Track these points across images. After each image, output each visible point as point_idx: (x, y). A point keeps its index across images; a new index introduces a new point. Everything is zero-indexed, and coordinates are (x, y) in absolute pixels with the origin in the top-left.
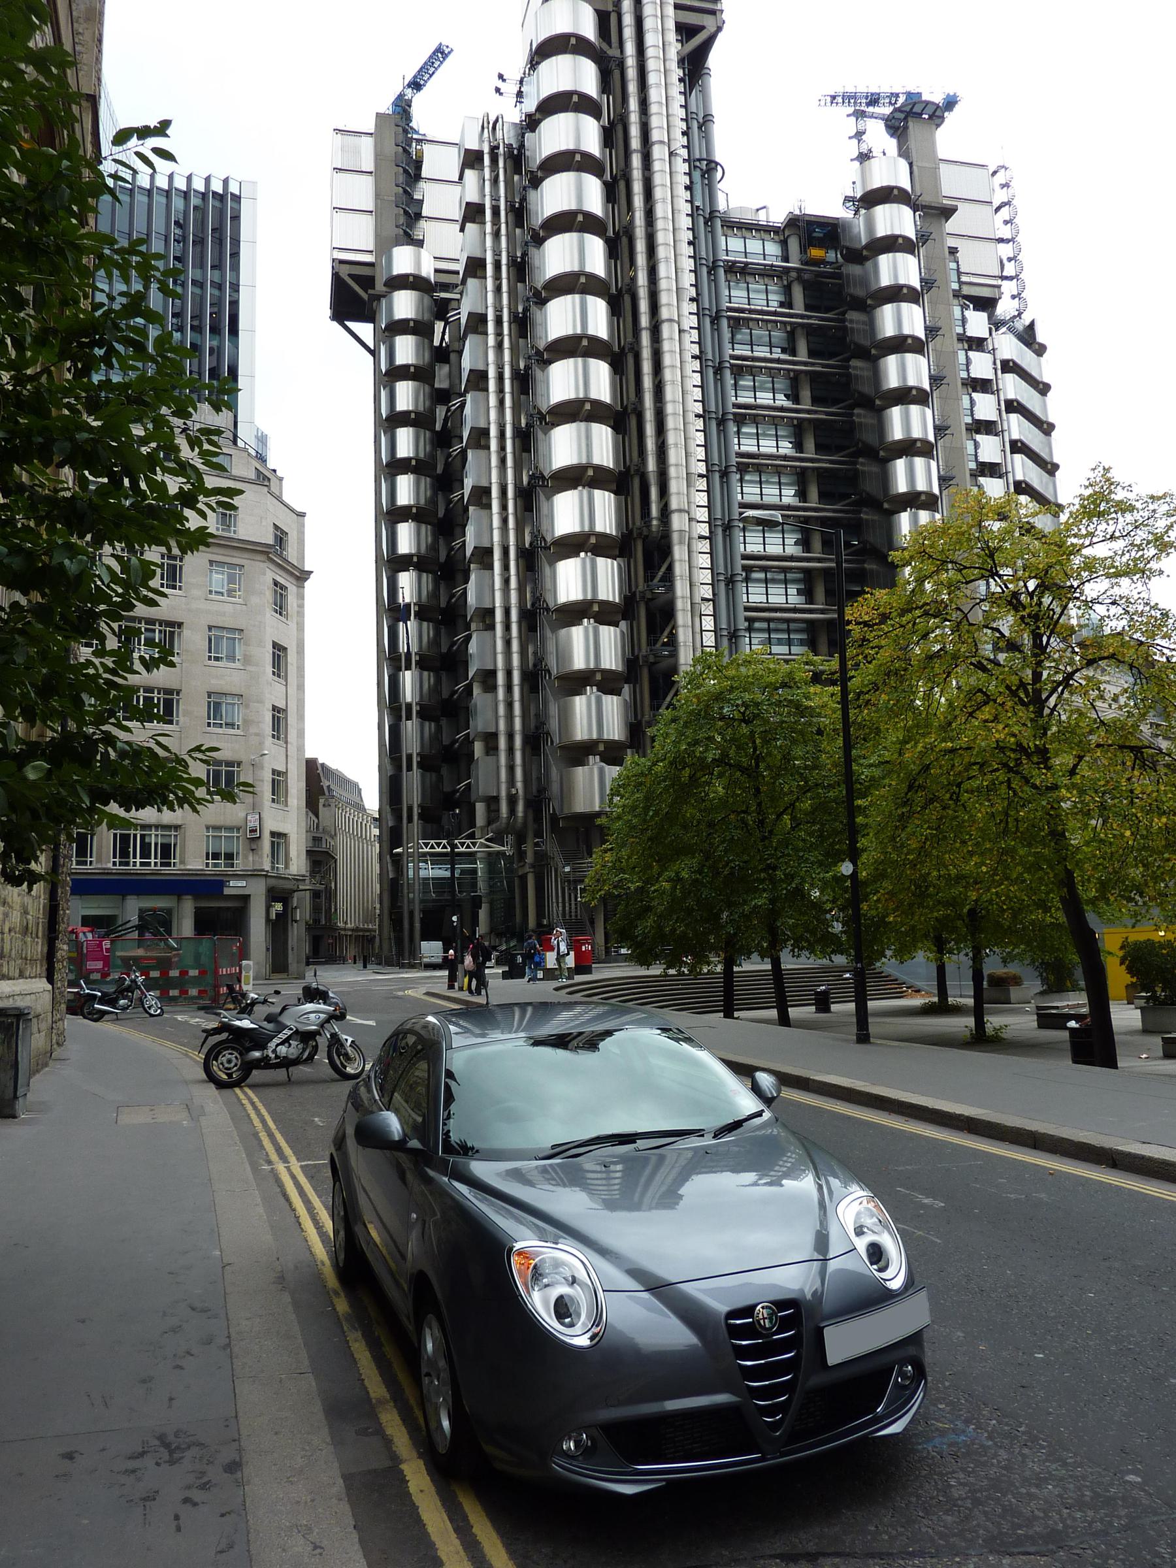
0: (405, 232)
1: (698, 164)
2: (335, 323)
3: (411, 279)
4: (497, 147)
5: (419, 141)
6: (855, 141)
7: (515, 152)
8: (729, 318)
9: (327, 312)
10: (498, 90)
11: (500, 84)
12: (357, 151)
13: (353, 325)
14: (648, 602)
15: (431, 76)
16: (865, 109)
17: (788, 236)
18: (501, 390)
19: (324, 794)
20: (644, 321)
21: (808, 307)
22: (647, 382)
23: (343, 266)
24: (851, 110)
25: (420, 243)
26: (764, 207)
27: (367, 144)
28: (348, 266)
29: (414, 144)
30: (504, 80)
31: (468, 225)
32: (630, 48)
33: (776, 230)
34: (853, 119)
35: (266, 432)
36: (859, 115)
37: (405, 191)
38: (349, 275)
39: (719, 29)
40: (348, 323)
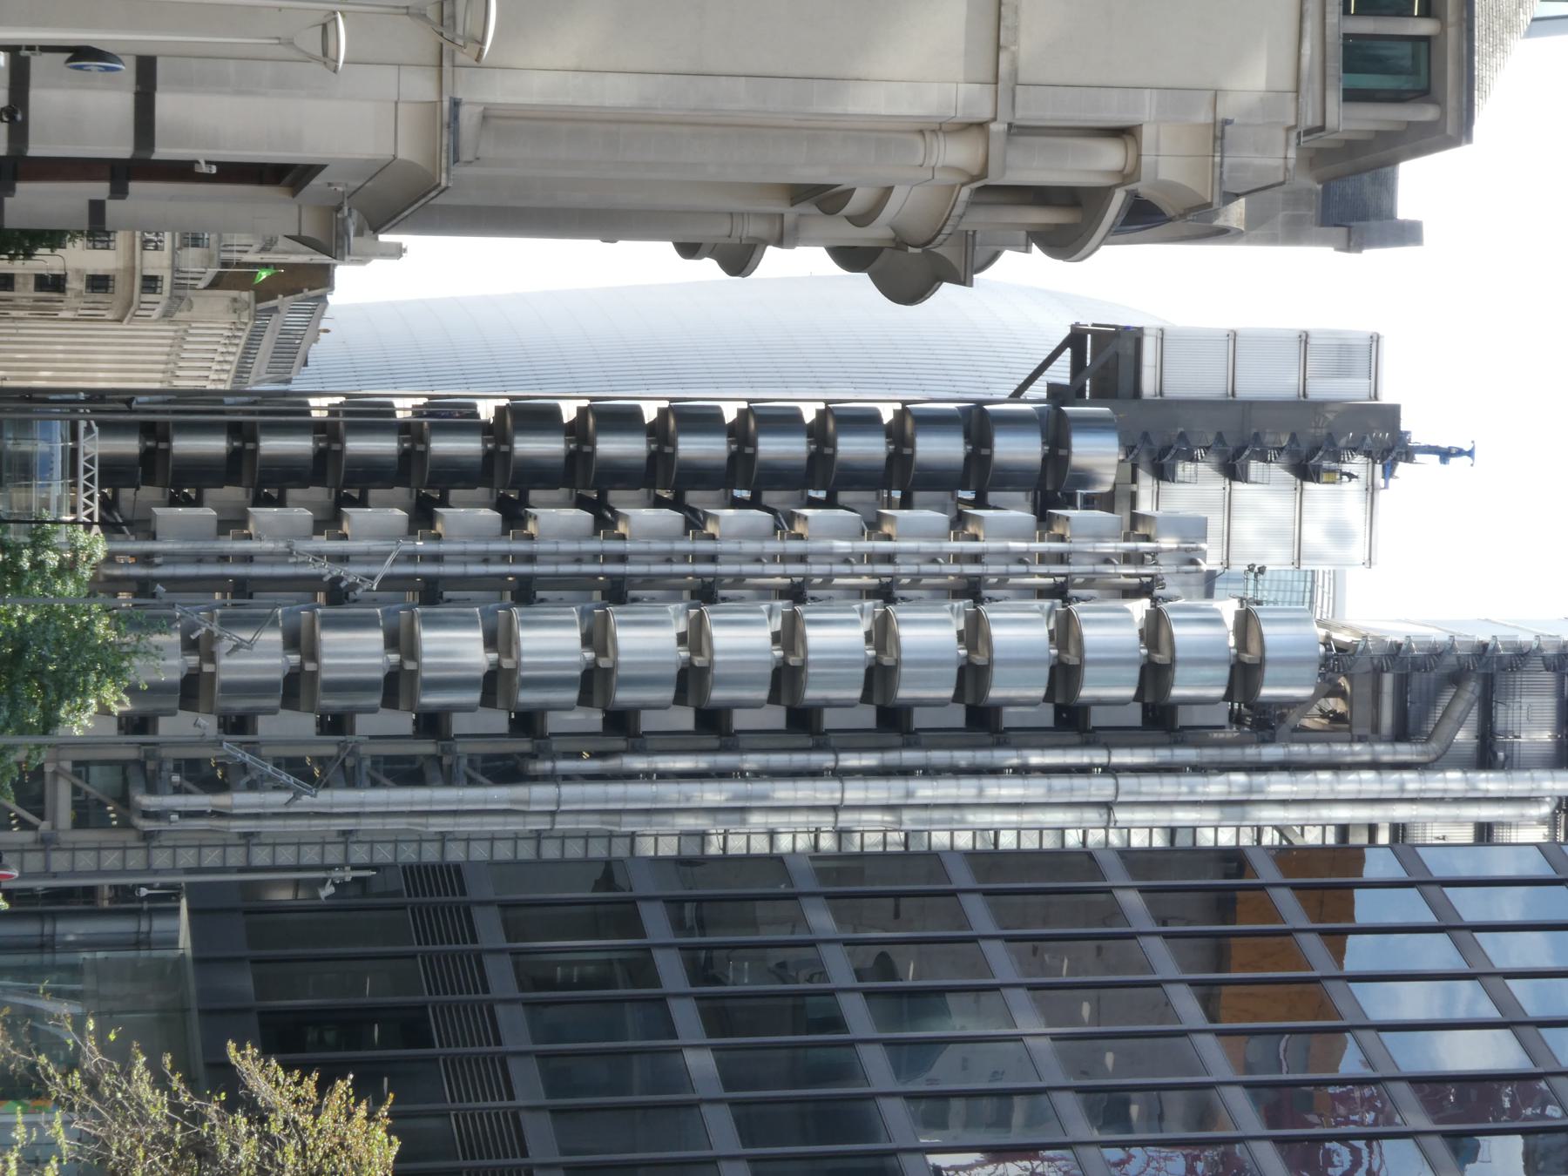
2: (1067, 332)
9: (1087, 320)
11: (1256, 569)
12: (1343, 371)
14: (437, 759)
19: (258, 300)
23: (1130, 346)
28: (1131, 351)
40: (1069, 350)
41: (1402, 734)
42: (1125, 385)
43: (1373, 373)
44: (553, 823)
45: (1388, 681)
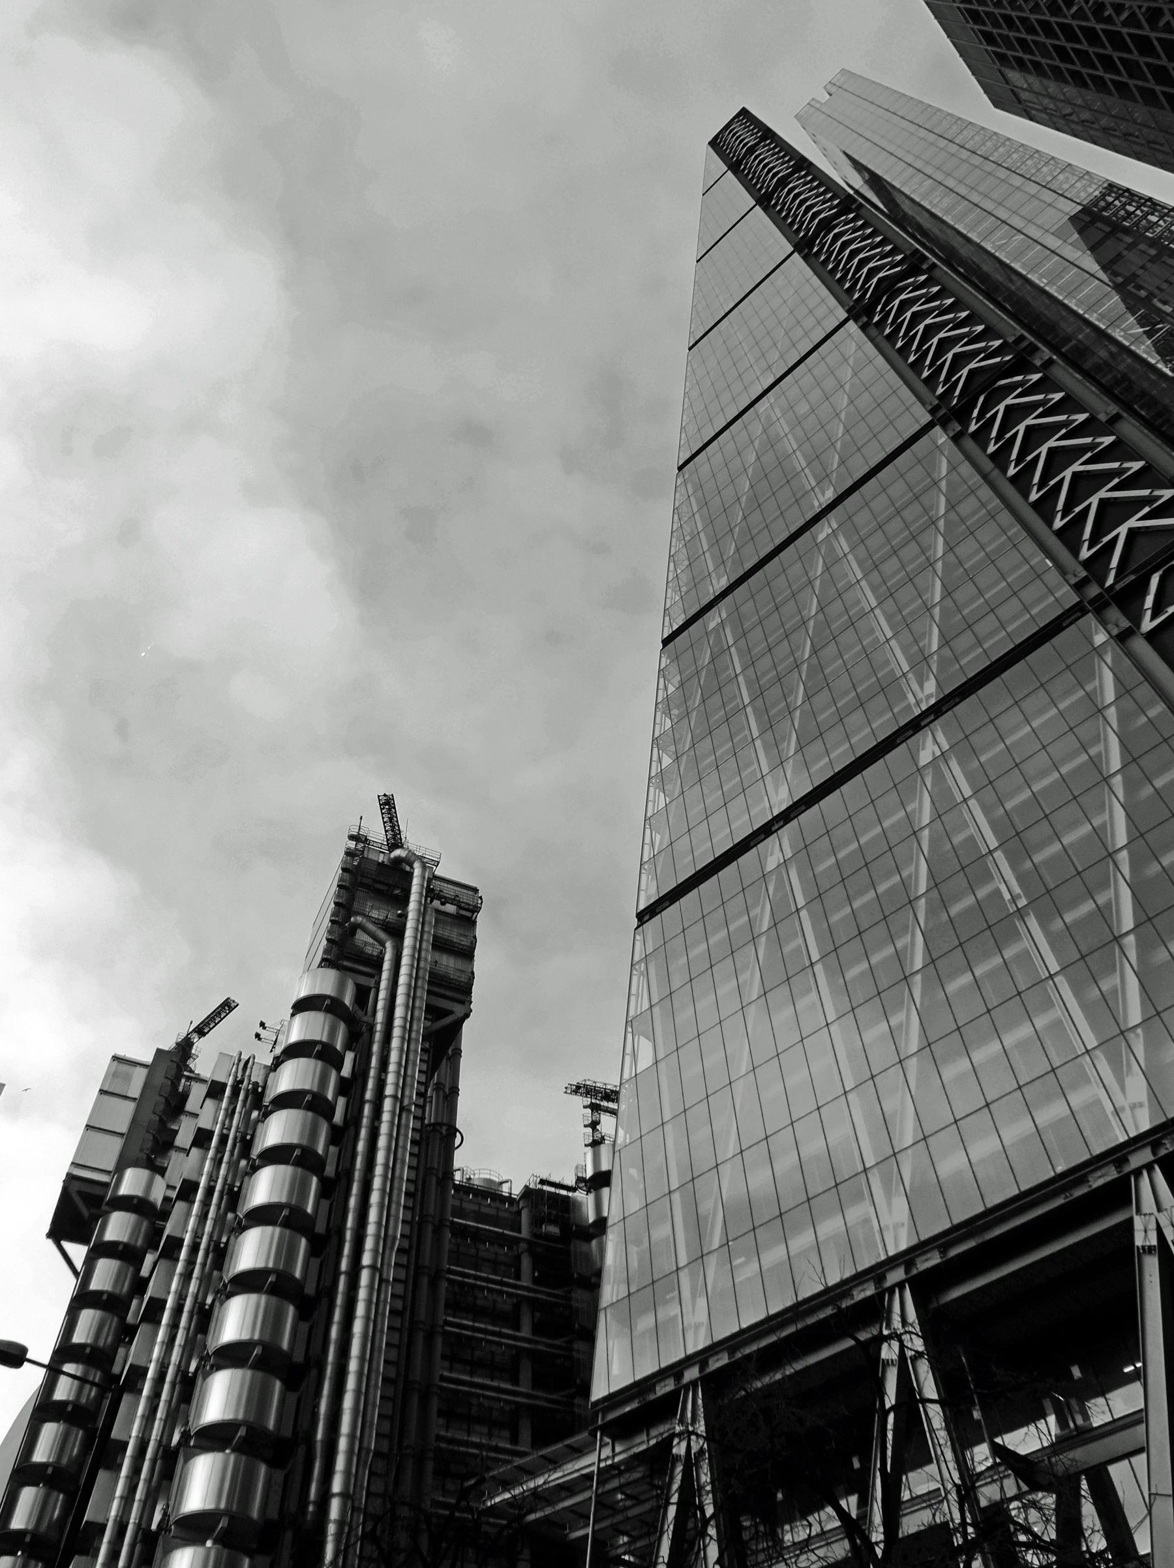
0: (149, 1158)
1: (438, 1128)
3: (135, 1201)
4: (242, 1082)
5: (188, 1078)
6: (589, 1130)
7: (260, 1090)
8: (449, 1280)
10: (258, 1036)
11: (260, 1030)
12: (128, 1078)
13: (67, 1245)
15: (216, 1024)
16: (602, 1103)
18: (174, 1326)
20: (344, 1265)
21: (535, 1281)
22: (334, 1332)
24: (588, 1101)
25: (162, 1171)
26: (507, 1182)
27: (140, 1075)
29: (183, 1081)
30: (264, 1028)
31: (193, 1149)
32: (380, 1017)
34: (589, 1111)
36: (595, 1108)
37: (161, 1120)
39: (467, 1016)
41: (377, 963)
42: (97, 1191)
44: (359, 1509)
45: (346, 963)
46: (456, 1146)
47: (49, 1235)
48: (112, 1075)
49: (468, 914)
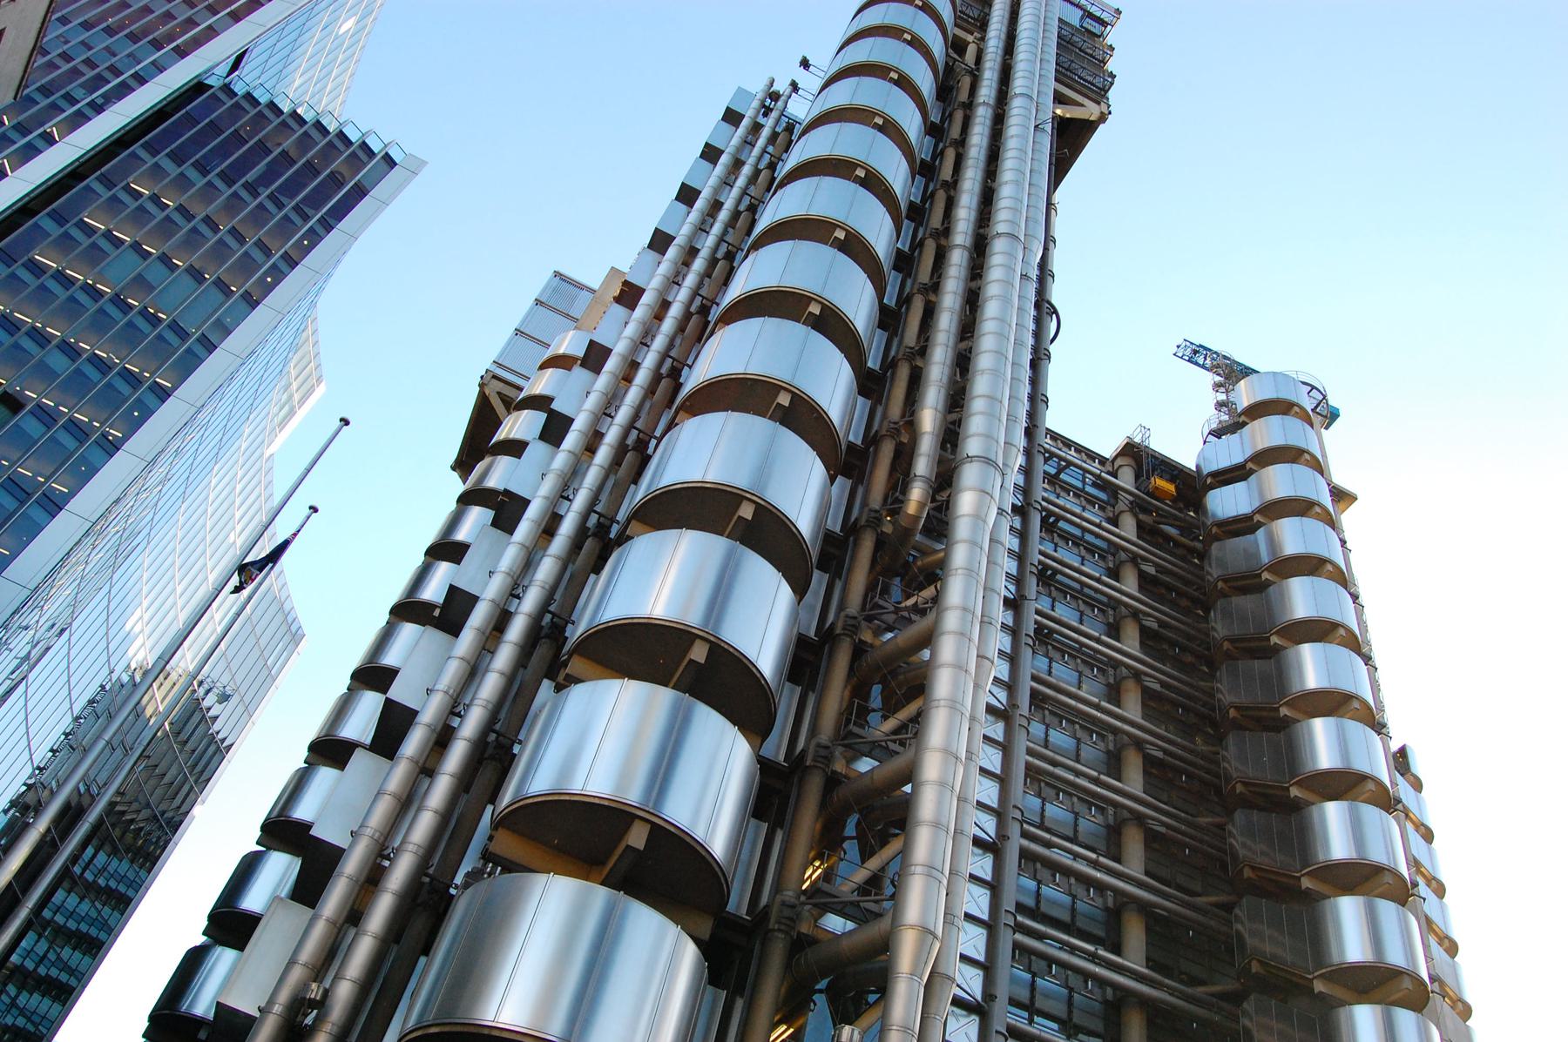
11: (802, 77)
17: (1120, 466)
33: (1103, 461)
35: (306, 629)
38: (499, 393)
39: (1103, 118)
43: (581, 287)
46: (1052, 336)
47: (454, 468)
48: (555, 290)
49: (1096, 28)
